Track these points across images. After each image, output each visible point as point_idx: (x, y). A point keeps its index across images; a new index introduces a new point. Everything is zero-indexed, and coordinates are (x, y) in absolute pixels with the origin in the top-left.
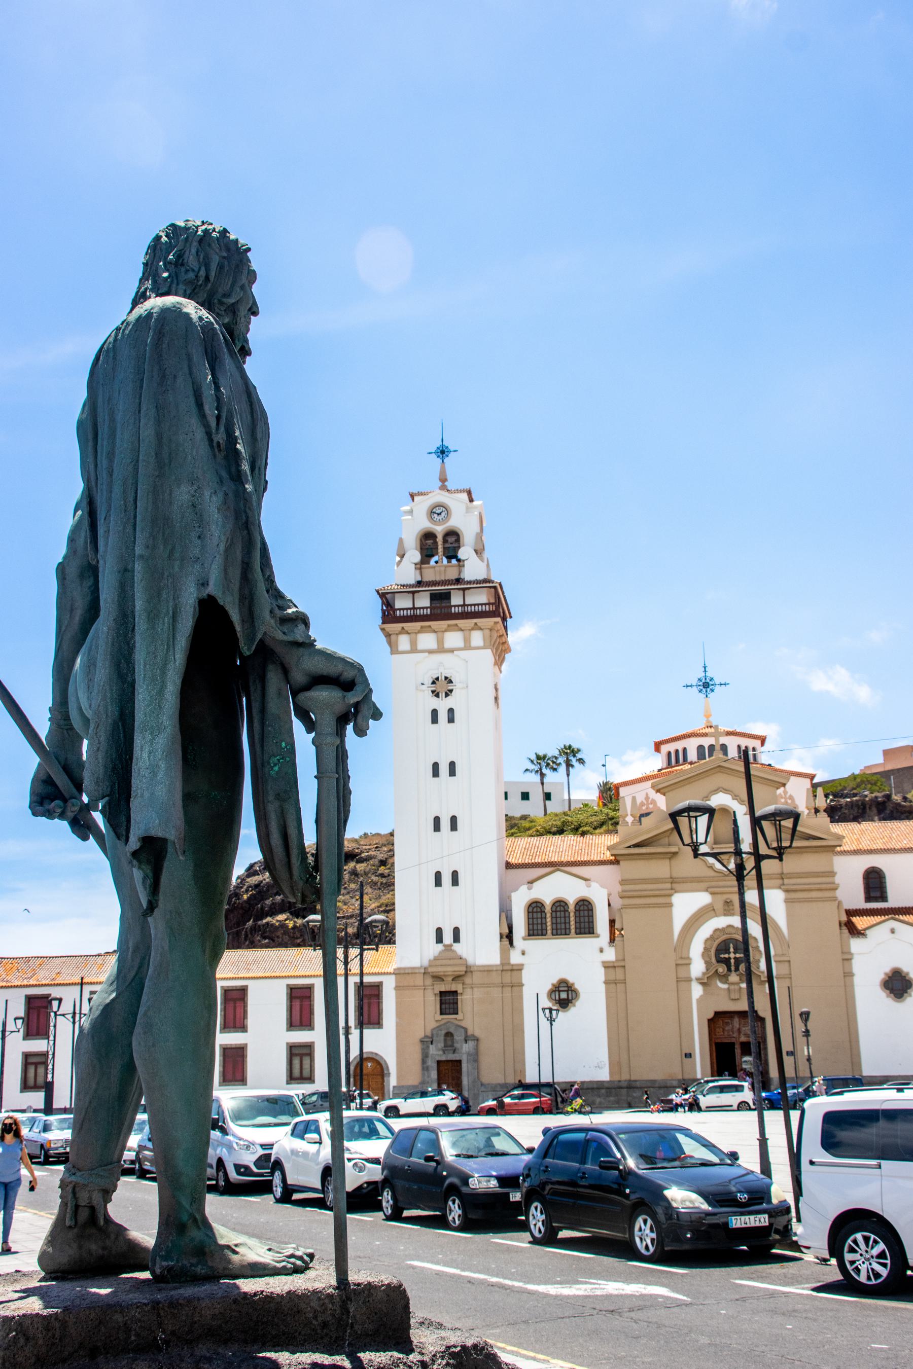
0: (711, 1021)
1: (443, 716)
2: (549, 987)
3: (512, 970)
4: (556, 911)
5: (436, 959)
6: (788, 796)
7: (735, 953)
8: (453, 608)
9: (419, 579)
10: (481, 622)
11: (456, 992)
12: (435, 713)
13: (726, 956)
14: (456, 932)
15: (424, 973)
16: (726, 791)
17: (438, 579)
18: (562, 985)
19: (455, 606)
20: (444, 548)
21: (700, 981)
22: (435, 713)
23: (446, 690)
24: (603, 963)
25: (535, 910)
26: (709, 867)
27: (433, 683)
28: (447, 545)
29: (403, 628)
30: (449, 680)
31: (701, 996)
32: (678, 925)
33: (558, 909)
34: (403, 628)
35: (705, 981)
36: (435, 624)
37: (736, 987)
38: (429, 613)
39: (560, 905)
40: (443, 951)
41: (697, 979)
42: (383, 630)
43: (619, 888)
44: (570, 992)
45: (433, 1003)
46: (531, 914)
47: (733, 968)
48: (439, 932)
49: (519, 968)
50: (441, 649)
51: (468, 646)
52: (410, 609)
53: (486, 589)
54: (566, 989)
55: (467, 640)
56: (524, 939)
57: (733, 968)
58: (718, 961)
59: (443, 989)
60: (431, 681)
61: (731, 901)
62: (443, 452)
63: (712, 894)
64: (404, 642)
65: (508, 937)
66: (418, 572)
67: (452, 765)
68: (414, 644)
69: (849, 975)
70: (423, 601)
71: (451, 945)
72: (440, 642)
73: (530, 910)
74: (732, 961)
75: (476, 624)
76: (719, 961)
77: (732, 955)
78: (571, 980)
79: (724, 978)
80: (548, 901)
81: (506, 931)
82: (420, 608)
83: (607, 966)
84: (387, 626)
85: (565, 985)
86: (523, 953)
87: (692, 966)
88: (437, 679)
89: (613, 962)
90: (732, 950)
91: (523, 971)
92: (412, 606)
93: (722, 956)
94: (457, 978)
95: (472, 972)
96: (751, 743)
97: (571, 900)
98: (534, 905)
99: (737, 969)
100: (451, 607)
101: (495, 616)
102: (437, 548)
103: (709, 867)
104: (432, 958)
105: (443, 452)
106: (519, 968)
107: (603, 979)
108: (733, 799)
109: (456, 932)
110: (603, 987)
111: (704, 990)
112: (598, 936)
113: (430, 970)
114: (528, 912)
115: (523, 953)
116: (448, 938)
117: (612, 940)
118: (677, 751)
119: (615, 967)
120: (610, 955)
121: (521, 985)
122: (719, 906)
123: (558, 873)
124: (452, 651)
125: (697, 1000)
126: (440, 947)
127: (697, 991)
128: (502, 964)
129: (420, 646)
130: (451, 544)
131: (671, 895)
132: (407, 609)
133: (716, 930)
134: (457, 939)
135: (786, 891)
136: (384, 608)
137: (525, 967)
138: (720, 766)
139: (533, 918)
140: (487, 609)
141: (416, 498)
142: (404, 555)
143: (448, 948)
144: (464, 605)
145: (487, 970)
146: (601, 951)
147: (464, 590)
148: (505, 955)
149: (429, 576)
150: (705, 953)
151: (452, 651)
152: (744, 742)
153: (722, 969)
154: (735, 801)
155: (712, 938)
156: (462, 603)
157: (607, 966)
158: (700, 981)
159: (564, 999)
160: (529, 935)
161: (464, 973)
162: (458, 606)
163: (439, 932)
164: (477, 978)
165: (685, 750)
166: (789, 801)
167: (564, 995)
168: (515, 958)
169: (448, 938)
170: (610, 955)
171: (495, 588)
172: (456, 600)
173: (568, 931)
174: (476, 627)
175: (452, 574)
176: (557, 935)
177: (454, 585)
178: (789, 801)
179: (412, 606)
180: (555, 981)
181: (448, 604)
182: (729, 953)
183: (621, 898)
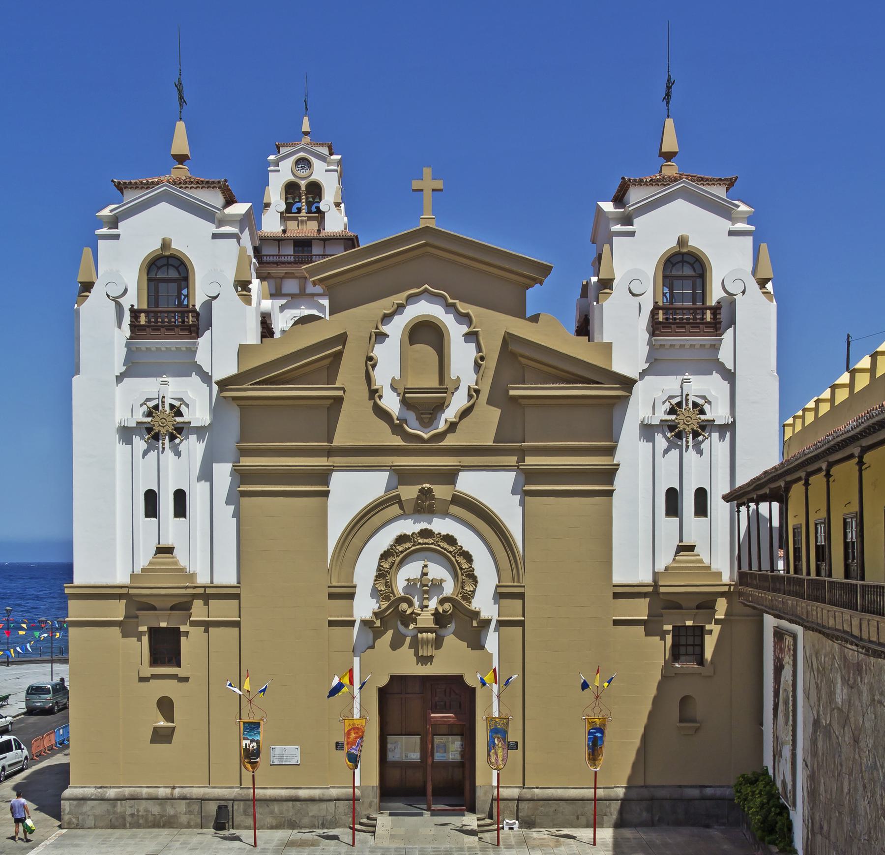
32: (336, 529)
37: (431, 636)
122: (409, 492)
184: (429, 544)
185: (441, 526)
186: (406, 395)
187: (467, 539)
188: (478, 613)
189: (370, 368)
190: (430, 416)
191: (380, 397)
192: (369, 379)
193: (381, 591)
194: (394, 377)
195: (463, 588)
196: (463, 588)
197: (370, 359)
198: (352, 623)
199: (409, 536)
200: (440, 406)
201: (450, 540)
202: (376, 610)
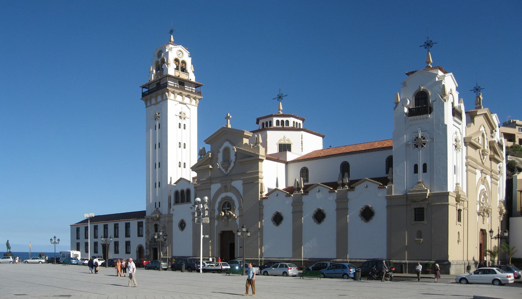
11: (157, 224)
31: (217, 225)
39: (182, 191)
45: (153, 229)
56: (173, 205)
65: (170, 205)
71: (158, 208)
80: (179, 190)
81: (169, 202)
94: (158, 219)
97: (185, 189)
108: (230, 144)
121: (172, 221)
125: (216, 226)
137: (174, 215)
155: (221, 202)
159: (183, 227)
164: (162, 220)
178: (287, 142)
185: (230, 194)
187: (234, 198)
200: (229, 167)
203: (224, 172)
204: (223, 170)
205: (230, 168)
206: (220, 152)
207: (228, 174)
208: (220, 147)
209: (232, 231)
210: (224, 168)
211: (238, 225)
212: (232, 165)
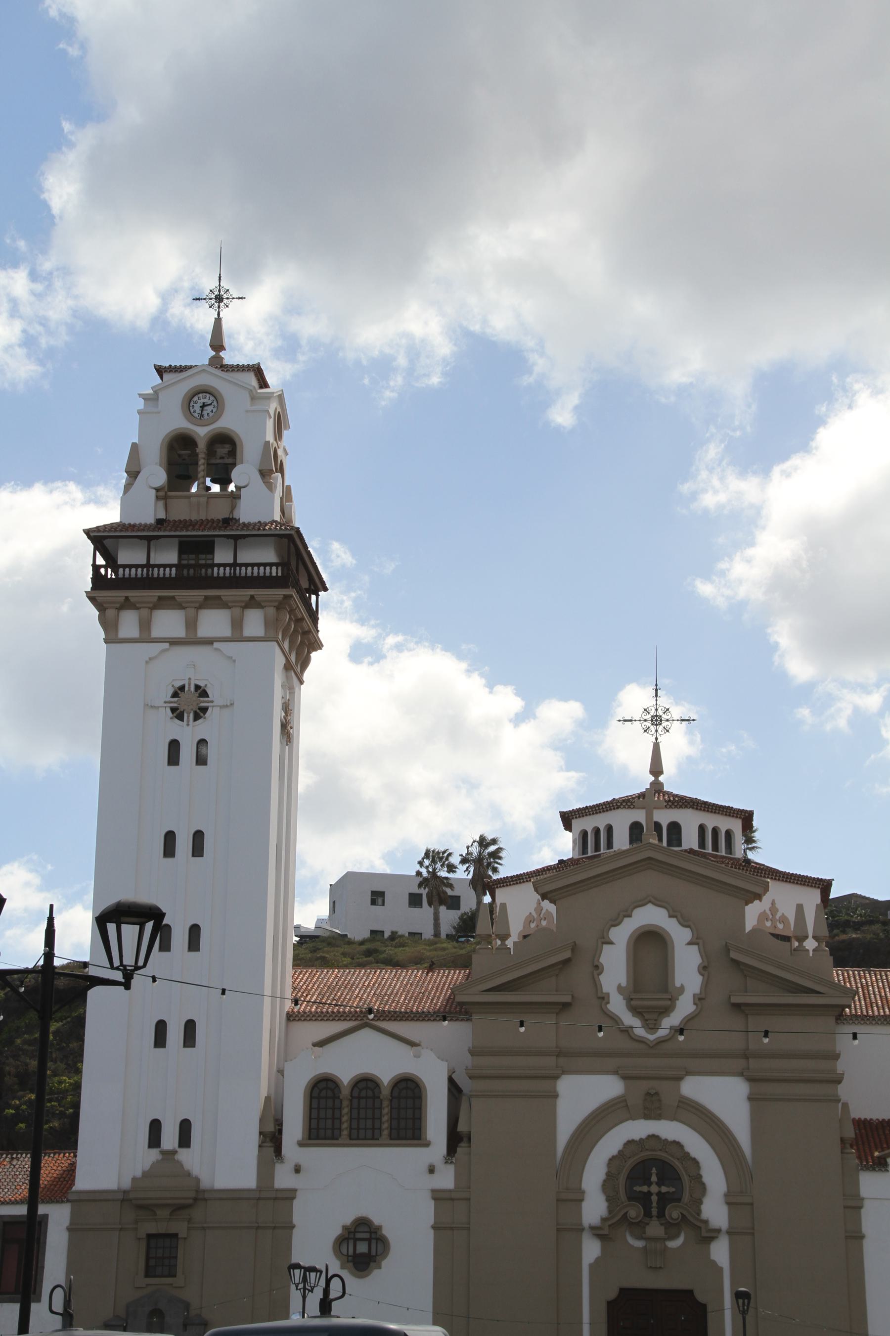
0: (611, 1305)
1: (187, 753)
2: (338, 1231)
3: (275, 1199)
4: (359, 1098)
5: (145, 1174)
6: (777, 917)
7: (659, 1184)
8: (216, 569)
9: (162, 515)
10: (260, 593)
11: (175, 1236)
12: (174, 747)
13: (645, 1189)
14: (185, 1127)
15: (123, 1201)
16: (658, 903)
17: (194, 517)
18: (361, 1229)
19: (219, 565)
20: (208, 464)
21: (597, 1232)
22: (174, 747)
23: (196, 708)
24: (433, 1191)
25: (323, 1094)
26: (622, 1031)
27: (175, 695)
28: (213, 461)
29: (127, 598)
30: (204, 694)
31: (597, 1260)
33: (363, 1094)
34: (127, 598)
35: (606, 1232)
36: (179, 594)
38: (173, 575)
40: (158, 1161)
41: (592, 1228)
42: (92, 599)
43: (468, 1060)
44: (374, 1242)
46: (315, 1102)
47: (654, 1212)
48: (155, 1127)
49: (289, 1196)
50: (192, 640)
51: (237, 635)
52: (142, 566)
53: (273, 538)
54: (367, 1236)
55: (237, 624)
56: (301, 1144)
57: (654, 1212)
58: (630, 1199)
59: (153, 1231)
60: (171, 692)
61: (657, 1094)
62: (219, 299)
63: (624, 1078)
64: (129, 623)
66: (161, 504)
67: (198, 837)
68: (145, 626)
69: (856, 1237)
70: (168, 556)
71: (174, 1152)
72: (191, 625)
73: (315, 1094)
74: (654, 1198)
75: (252, 597)
76: (633, 1197)
77: (654, 1189)
78: (376, 1221)
79: (638, 1228)
80: (346, 1076)
82: (159, 566)
83: (438, 1196)
84: (99, 594)
85: (367, 1229)
86: (297, 1170)
87: (585, 1205)
88: (182, 688)
89: (450, 1191)
90: (654, 1178)
91: (295, 1202)
92: (145, 562)
93: (637, 1188)
94: (179, 1209)
95: (205, 1200)
96: (724, 824)
97: (386, 1076)
98: (323, 1085)
99: (661, 1215)
100: (213, 565)
101: (285, 586)
102: (196, 464)
103: (622, 1031)
104: (139, 1174)
105: (219, 299)
106: (289, 1196)
107: (432, 1222)
108: (670, 916)
109: (185, 1127)
110: (430, 1236)
111: (603, 1249)
112: (427, 1144)
113: (132, 1196)
114: (311, 1097)
115: (297, 1170)
116: (170, 1138)
117: (452, 1149)
118: (597, 831)
119: (452, 1199)
120: (446, 1179)
123: (366, 1033)
124: (209, 642)
125: (591, 1266)
126: (154, 1154)
127: (591, 1250)
128: (259, 1189)
129: (156, 633)
130: (222, 458)
131: (556, 1077)
132: (137, 566)
133: (630, 1143)
134: (185, 1139)
135: (751, 1080)
136: (100, 561)
137: (298, 1193)
138: (650, 858)
139: (319, 1108)
140: (274, 574)
141: (165, 376)
142: (139, 472)
143: (169, 1155)
144: (235, 565)
145: (234, 1196)
146: (432, 1170)
147: (236, 538)
148: (265, 1170)
149: (181, 511)
150: (608, 1185)
151: (209, 642)
152: (711, 821)
153: (634, 1212)
154: (674, 921)
156: (231, 561)
157: (438, 1196)
158: (597, 1232)
159: (362, 1255)
160: (310, 1138)
161: (191, 1201)
162: (225, 565)
163: (155, 1127)
165: (609, 829)
166: (780, 926)
167: (362, 1248)
168: (283, 1179)
169: (170, 1138)
170: (446, 1179)
171: (289, 537)
172: (223, 555)
173: (377, 1132)
174: (253, 603)
175: (219, 512)
176: (358, 1139)
177: (220, 530)
178: (780, 926)
179: (145, 562)
180: (348, 1220)
181: (209, 562)
182: (650, 1184)
183: (470, 1078)
184: (654, 1150)
186: (633, 1003)
188: (706, 1222)
189: (596, 976)
190: (655, 1022)
191: (608, 1003)
192: (596, 985)
193: (609, 1196)
194: (620, 984)
195: (691, 1196)
196: (691, 1196)
197: (597, 967)
198: (583, 1230)
199: (637, 1141)
200: (666, 1011)
201: (678, 1144)
202: (604, 1216)
203: (640, 1032)
204: (629, 1020)
205: (674, 1019)
206: (611, 943)
207: (661, 1042)
208: (616, 922)
209: (690, 1292)
210: (636, 1011)
211: (720, 1270)
212: (684, 1007)
